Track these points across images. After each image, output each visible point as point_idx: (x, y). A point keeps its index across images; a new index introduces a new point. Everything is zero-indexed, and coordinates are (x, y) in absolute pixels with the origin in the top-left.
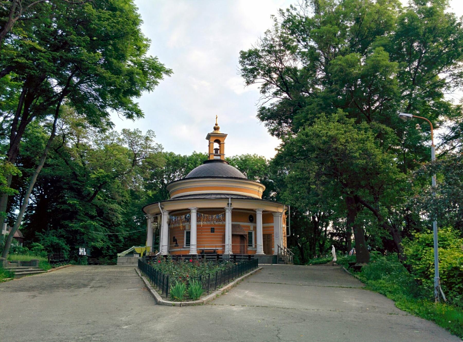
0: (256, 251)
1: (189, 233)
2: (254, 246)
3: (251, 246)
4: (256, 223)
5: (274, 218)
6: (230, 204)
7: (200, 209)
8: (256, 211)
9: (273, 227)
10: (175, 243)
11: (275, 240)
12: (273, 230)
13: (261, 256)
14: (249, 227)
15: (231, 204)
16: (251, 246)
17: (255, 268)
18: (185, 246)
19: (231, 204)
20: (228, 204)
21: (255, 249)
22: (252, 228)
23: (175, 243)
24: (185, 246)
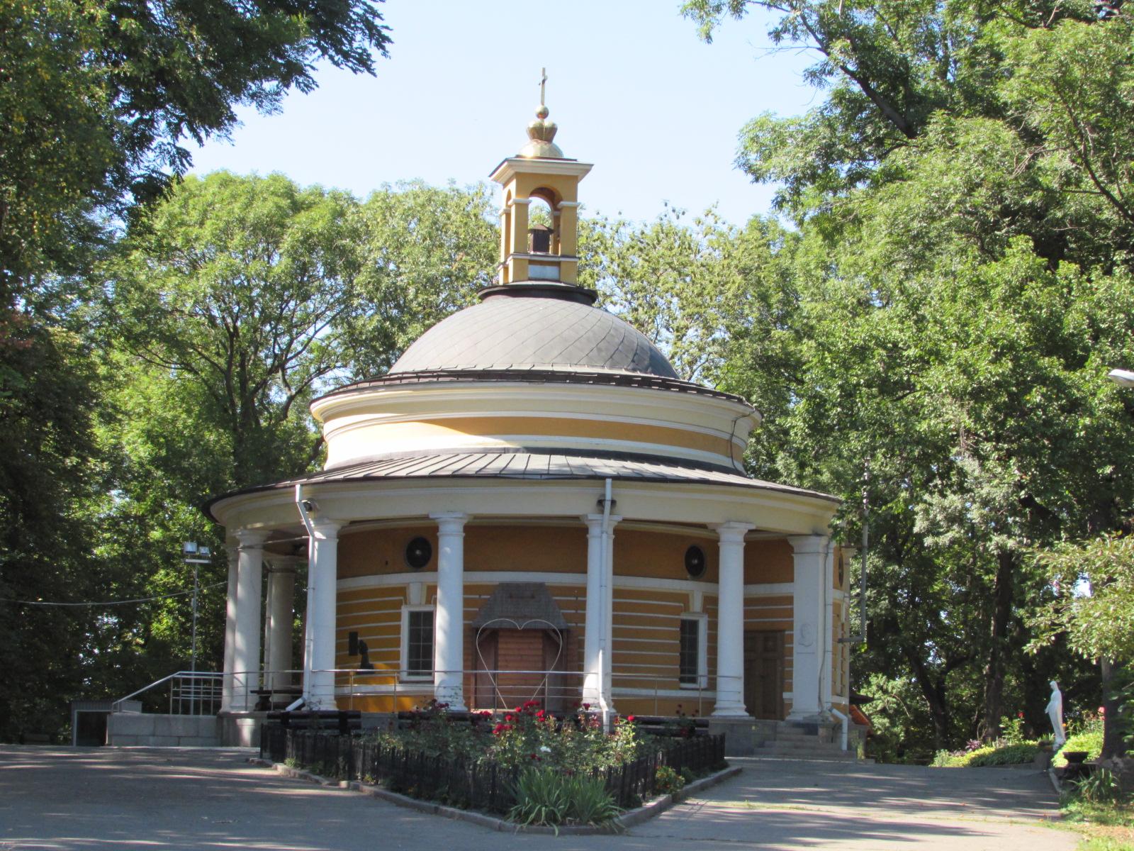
0: (710, 705)
1: (423, 625)
2: (703, 682)
3: (694, 680)
4: (715, 579)
5: (797, 560)
6: (608, 505)
7: (476, 517)
8: (719, 530)
9: (789, 600)
10: (360, 656)
11: (796, 658)
12: (790, 613)
13: (733, 724)
14: (684, 598)
15: (613, 502)
16: (694, 680)
17: (714, 770)
18: (404, 677)
19: (613, 502)
20: (601, 503)
21: (708, 694)
22: (697, 604)
23: (360, 656)
24: (404, 677)
